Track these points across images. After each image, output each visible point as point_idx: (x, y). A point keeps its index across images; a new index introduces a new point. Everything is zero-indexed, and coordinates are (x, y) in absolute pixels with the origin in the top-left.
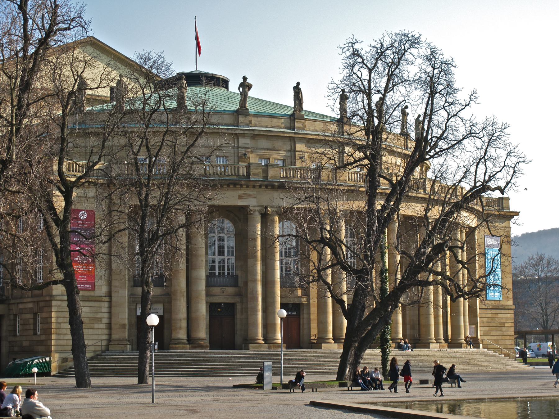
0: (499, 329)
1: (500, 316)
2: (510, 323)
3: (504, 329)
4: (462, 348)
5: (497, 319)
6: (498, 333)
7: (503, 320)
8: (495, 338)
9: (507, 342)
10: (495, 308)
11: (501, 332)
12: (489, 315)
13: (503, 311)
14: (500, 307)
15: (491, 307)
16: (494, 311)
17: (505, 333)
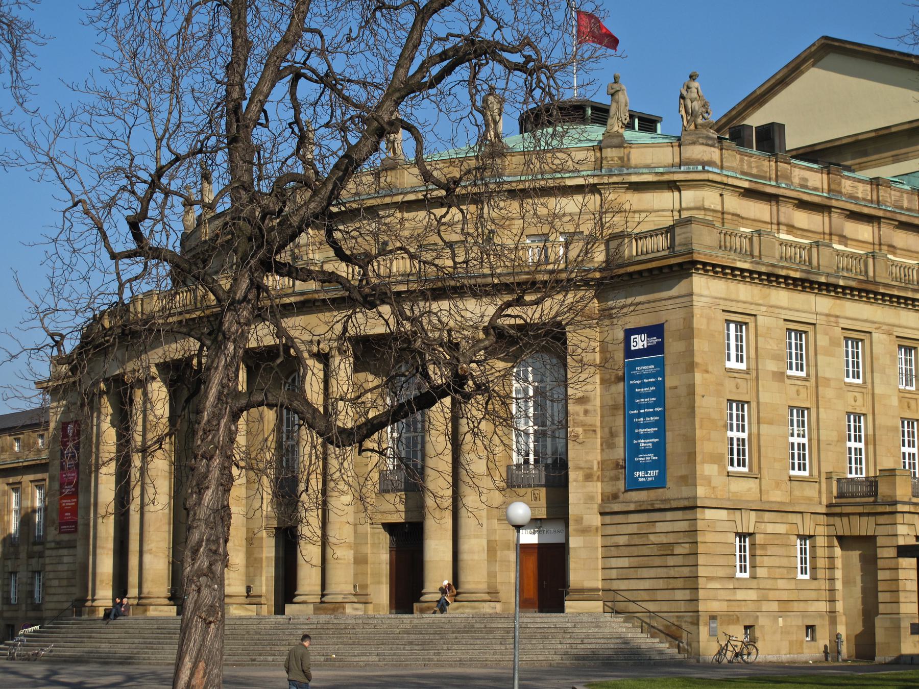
0: (657, 561)
1: (660, 527)
2: (687, 545)
3: (671, 561)
4: (412, 613)
5: (652, 537)
6: (651, 573)
7: (670, 539)
8: (646, 584)
9: (679, 595)
10: (643, 508)
11: (665, 570)
12: (633, 529)
13: (669, 515)
14: (657, 506)
15: (632, 507)
16: (643, 517)
17: (673, 572)
